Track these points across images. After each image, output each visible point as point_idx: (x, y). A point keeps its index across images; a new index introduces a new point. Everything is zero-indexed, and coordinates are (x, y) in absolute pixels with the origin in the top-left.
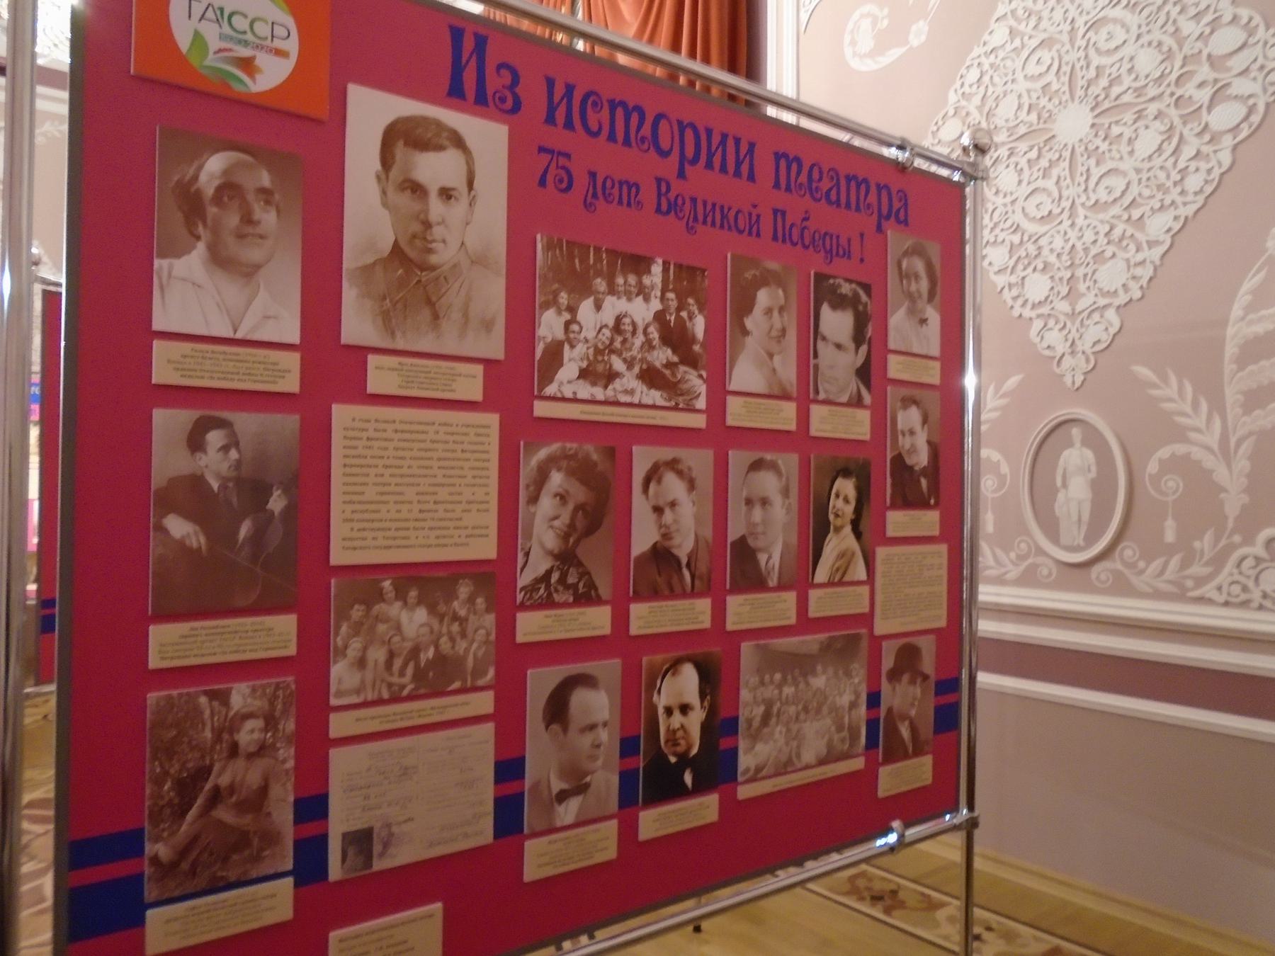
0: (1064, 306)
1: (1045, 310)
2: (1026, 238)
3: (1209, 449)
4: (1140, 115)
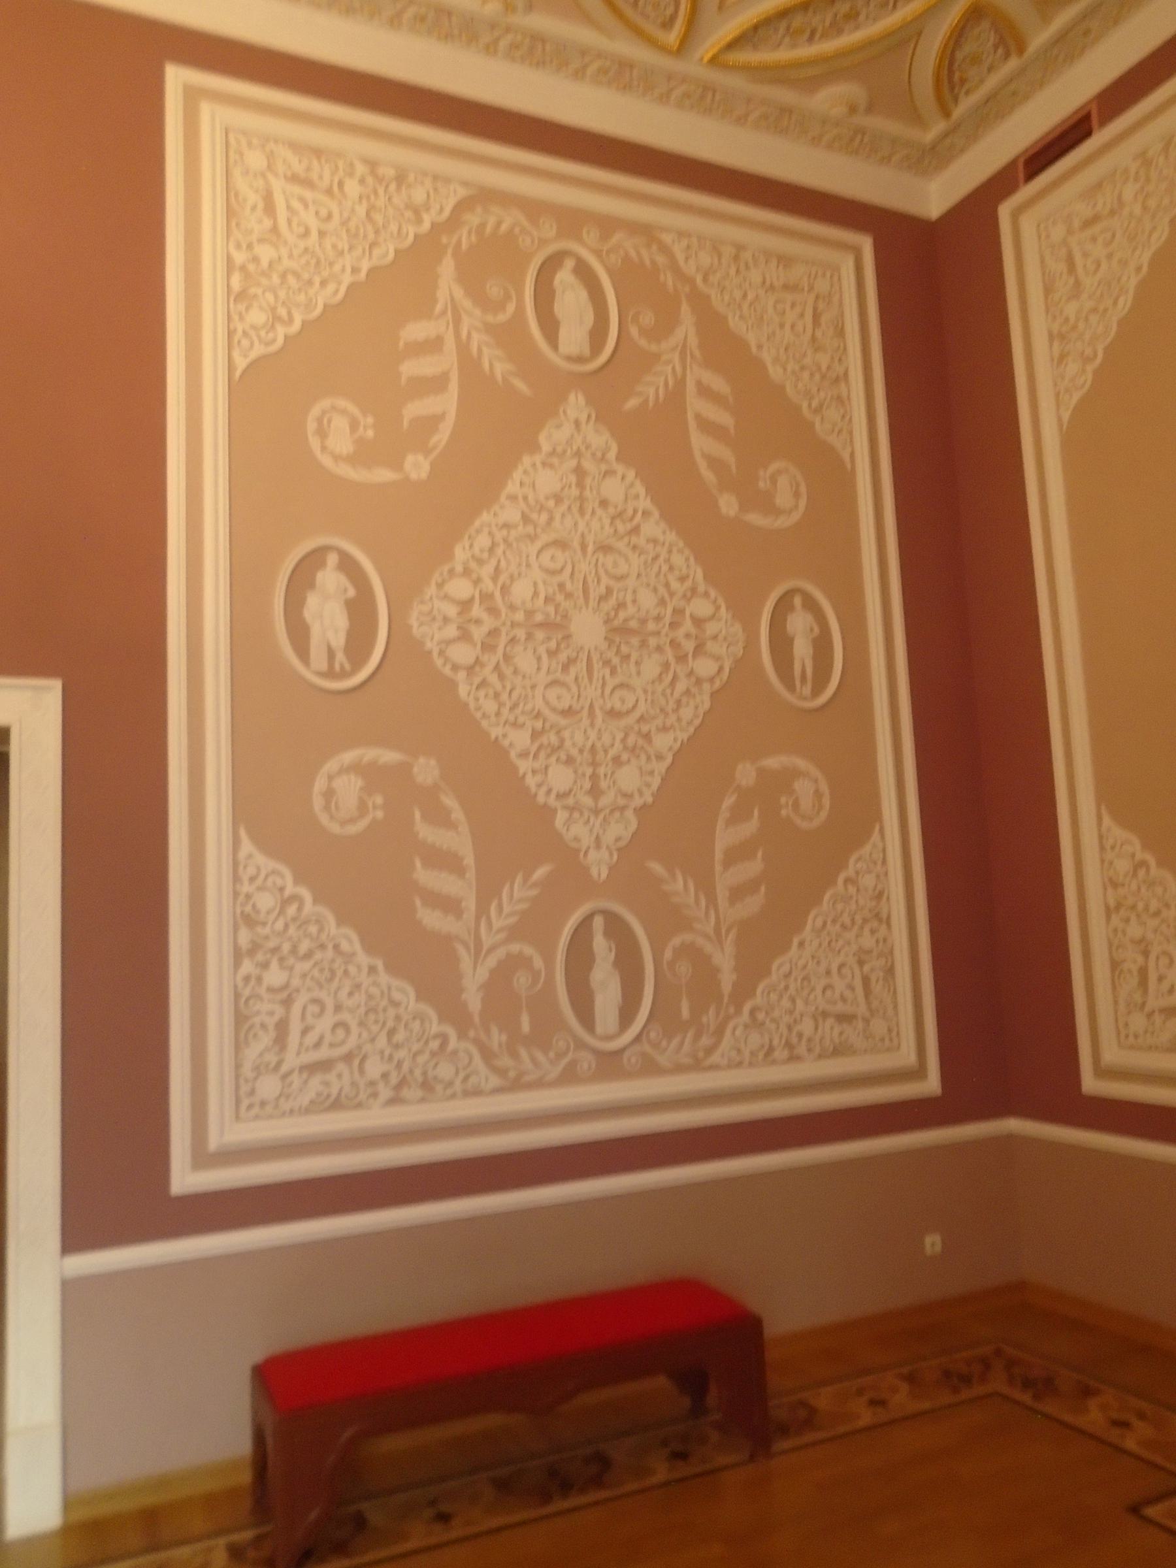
0: (588, 801)
1: (570, 801)
2: (547, 725)
3: (706, 936)
4: (644, 644)
